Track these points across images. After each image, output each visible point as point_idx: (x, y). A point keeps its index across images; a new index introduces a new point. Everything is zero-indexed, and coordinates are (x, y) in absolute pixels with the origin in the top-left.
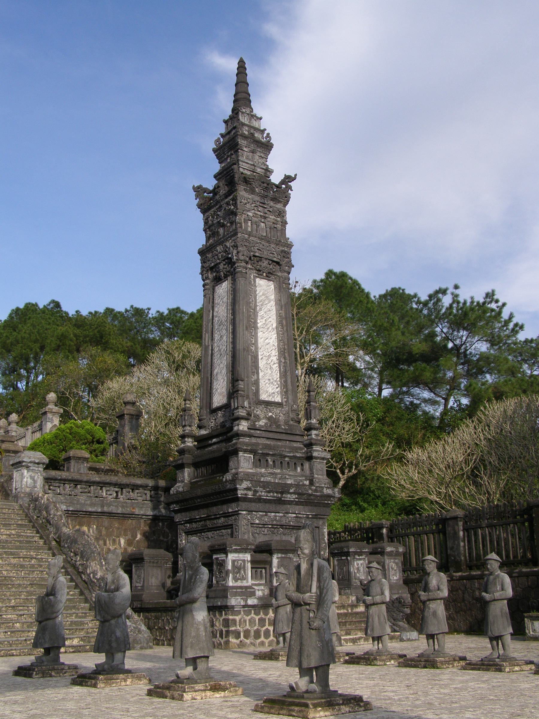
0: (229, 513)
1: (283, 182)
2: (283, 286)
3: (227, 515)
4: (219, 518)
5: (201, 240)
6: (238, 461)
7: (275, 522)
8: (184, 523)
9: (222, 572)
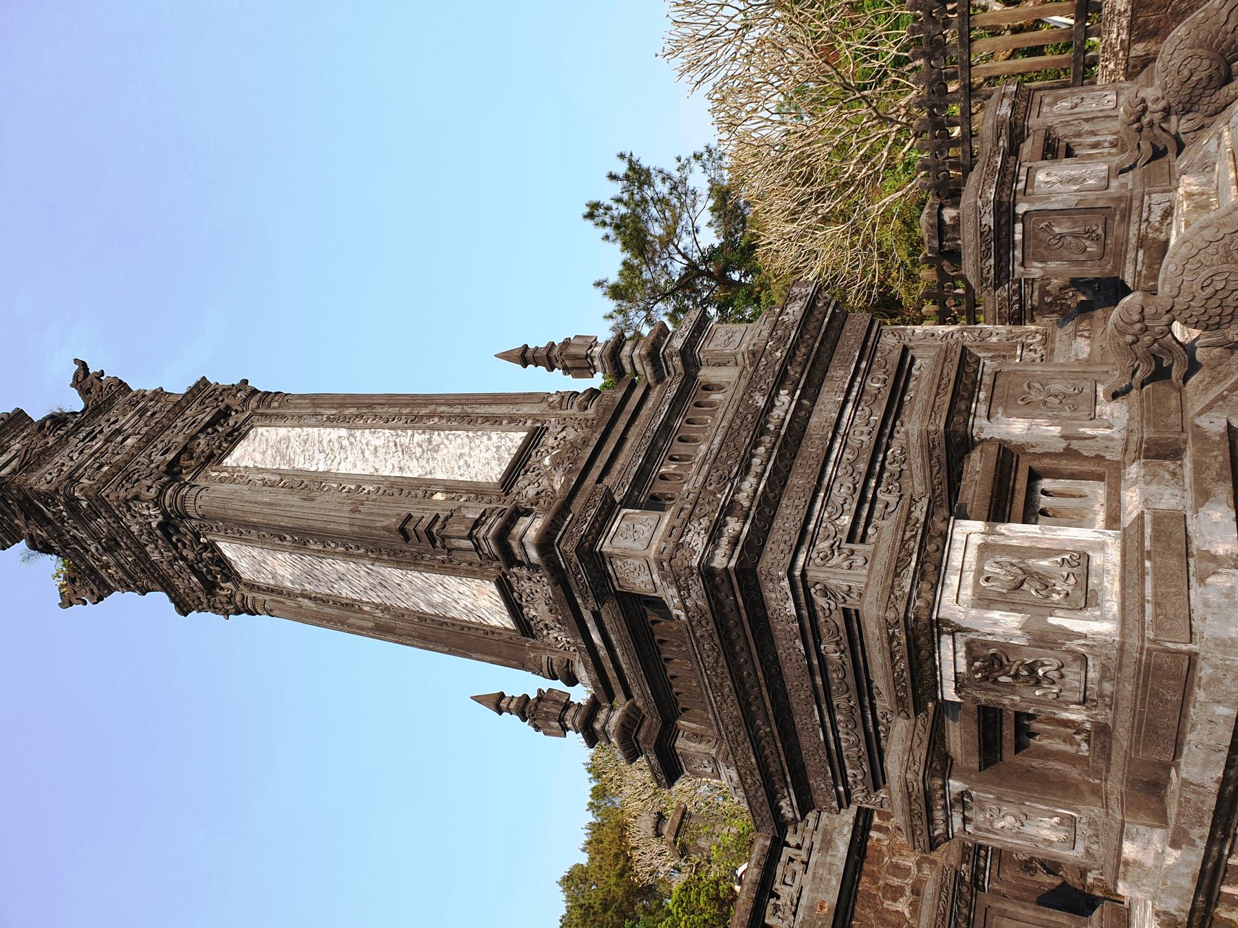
0: (800, 617)
1: (85, 392)
2: (274, 408)
4: (821, 658)
6: (624, 556)
7: (862, 467)
8: (845, 784)
9: (1032, 668)
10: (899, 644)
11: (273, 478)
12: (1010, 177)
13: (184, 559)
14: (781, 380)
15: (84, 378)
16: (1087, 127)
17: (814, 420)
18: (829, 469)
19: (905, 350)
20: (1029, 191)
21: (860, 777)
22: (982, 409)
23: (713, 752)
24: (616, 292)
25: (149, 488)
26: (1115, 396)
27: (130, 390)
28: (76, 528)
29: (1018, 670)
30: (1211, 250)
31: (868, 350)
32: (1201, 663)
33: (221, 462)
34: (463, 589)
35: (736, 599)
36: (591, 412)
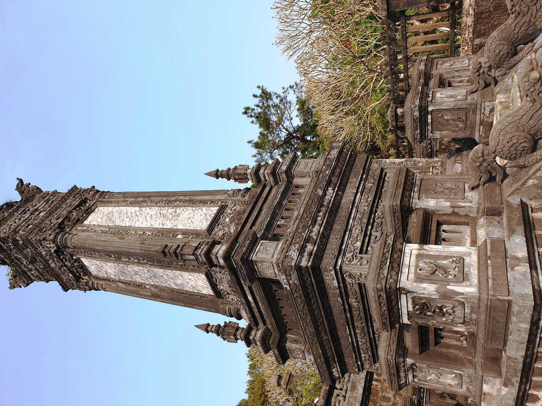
0: (339, 287)
1: (21, 192)
2: (107, 198)
4: (349, 305)
6: (262, 262)
7: (365, 220)
8: (361, 361)
9: (441, 308)
10: (383, 299)
11: (106, 229)
12: (425, 95)
13: (66, 266)
14: (329, 183)
15: (21, 186)
16: (457, 74)
17: (343, 201)
18: (351, 222)
19: (382, 169)
20: (433, 101)
21: (367, 358)
22: (416, 195)
23: (303, 348)
24: (257, 145)
25: (50, 235)
26: (473, 189)
27: (42, 191)
28: (17, 253)
29: (435, 309)
30: (510, 126)
31: (366, 170)
32: (513, 305)
33: (83, 223)
34: (190, 277)
35: (311, 280)
36: (247, 198)
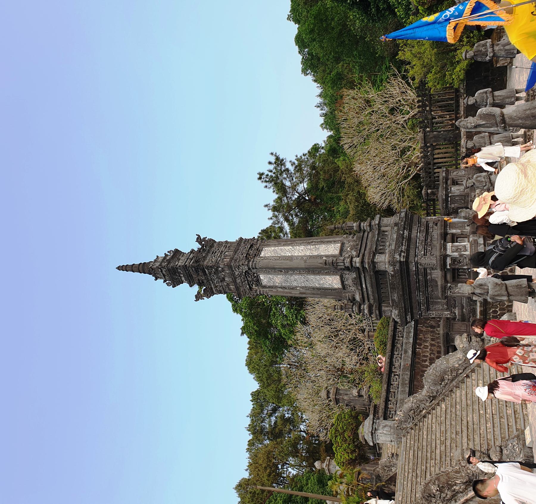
1: (200, 243)
3: (417, 273)
5: (229, 304)
7: (424, 243)
9: (459, 260)
11: (277, 258)
13: (248, 281)
14: (404, 228)
15: (199, 240)
16: (460, 178)
22: (449, 229)
24: (275, 209)
26: (468, 226)
34: (330, 279)
36: (355, 238)
